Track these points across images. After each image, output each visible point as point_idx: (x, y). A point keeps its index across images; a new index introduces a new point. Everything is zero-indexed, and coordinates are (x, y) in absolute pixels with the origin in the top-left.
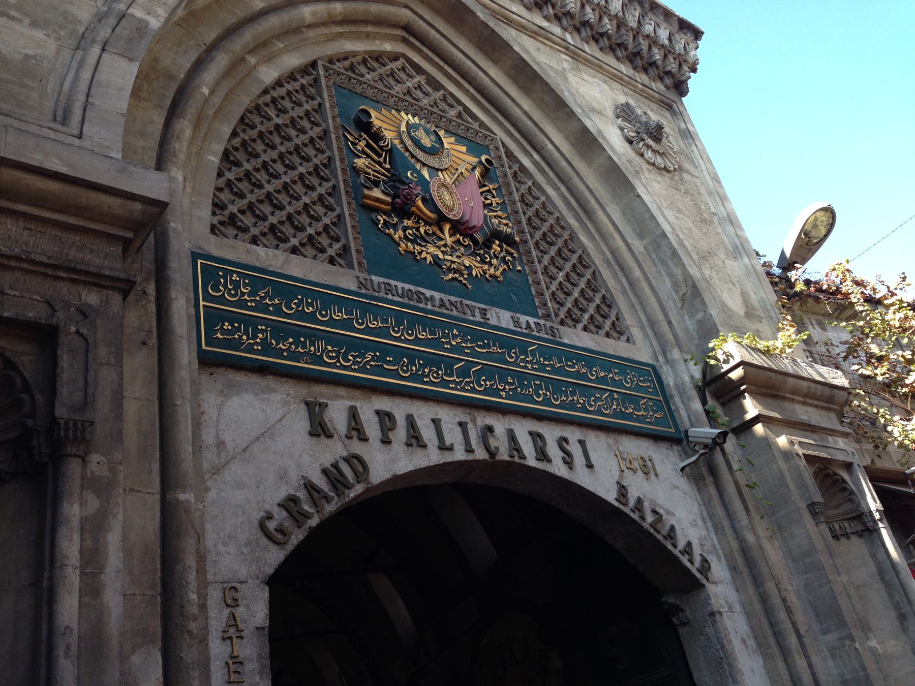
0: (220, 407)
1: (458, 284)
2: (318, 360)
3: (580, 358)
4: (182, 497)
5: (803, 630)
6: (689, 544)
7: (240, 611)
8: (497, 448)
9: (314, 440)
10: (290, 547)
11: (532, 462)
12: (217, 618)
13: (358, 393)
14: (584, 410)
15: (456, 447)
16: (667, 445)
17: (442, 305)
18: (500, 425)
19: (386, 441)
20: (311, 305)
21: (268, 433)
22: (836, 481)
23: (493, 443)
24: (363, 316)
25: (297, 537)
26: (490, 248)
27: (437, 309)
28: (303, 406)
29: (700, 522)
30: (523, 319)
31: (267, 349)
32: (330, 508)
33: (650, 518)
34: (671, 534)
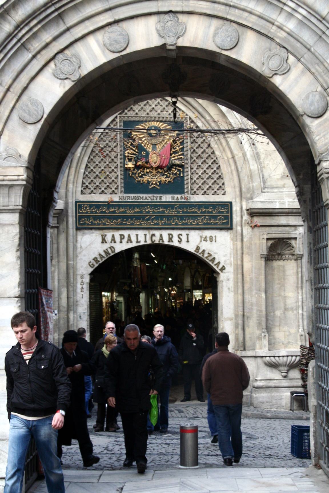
0: (81, 239)
1: (154, 188)
2: (105, 224)
3: (195, 206)
4: (70, 262)
5: (246, 288)
6: (219, 263)
7: (84, 280)
8: (155, 240)
9: (103, 244)
10: (94, 268)
11: (166, 242)
12: (79, 280)
13: (115, 231)
14: (191, 224)
15: (141, 241)
16: (226, 231)
17: (146, 199)
18: (157, 233)
19: (121, 242)
20: (104, 209)
21: (91, 243)
22: (288, 243)
23: (154, 238)
24: (119, 208)
25: (96, 265)
26: (170, 170)
27: (144, 201)
28: (100, 236)
29: (229, 255)
30: (176, 196)
31: (92, 224)
32: (104, 260)
33: (206, 255)
34: (213, 260)
